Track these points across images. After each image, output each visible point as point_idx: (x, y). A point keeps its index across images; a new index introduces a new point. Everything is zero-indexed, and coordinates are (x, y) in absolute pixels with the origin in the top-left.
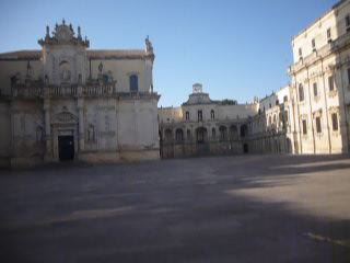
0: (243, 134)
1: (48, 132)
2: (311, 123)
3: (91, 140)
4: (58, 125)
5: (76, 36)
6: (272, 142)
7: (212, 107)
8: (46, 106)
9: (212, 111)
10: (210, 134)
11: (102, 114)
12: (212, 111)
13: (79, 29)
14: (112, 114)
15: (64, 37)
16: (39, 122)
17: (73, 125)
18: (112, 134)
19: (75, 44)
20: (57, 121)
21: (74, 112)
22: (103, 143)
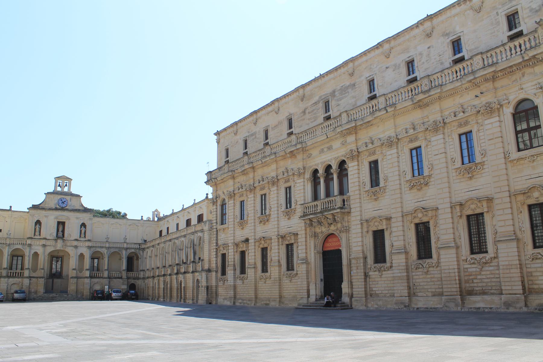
0: (130, 266)
6: (175, 285)
7: (85, 218)
9: (83, 225)
10: (73, 263)
12: (83, 225)
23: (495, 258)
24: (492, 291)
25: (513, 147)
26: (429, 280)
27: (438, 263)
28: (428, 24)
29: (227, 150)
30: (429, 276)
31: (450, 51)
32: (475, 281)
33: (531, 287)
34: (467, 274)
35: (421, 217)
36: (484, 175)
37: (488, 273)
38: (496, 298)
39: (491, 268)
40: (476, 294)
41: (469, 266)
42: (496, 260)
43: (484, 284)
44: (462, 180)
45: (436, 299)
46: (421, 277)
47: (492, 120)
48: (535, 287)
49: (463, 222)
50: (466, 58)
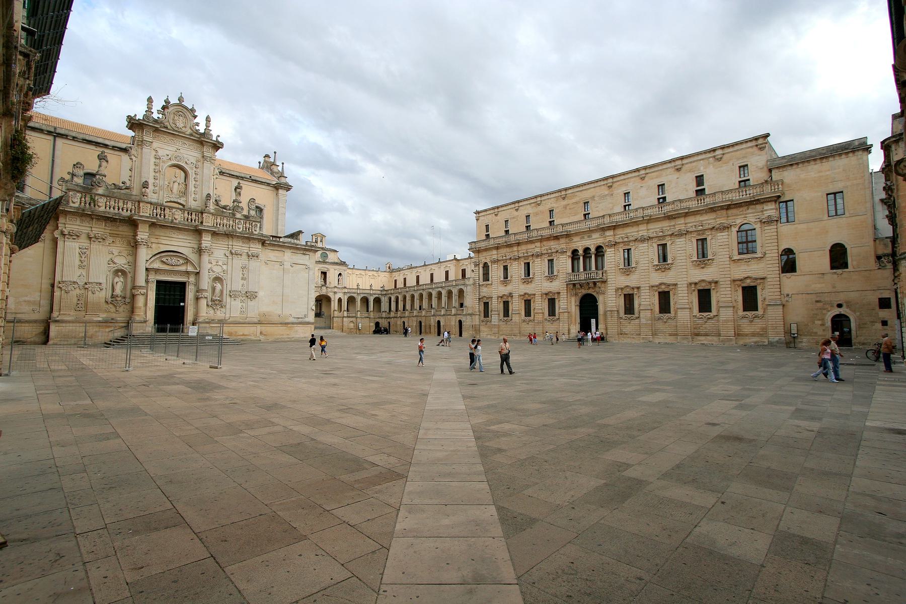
1: (141, 281)
2: (496, 306)
3: (217, 303)
4: (157, 271)
5: (201, 128)
8: (143, 234)
11: (238, 262)
13: (208, 119)
14: (253, 264)
15: (180, 124)
16: (122, 262)
17: (187, 273)
18: (251, 296)
19: (202, 143)
20: (157, 265)
21: (193, 257)
22: (234, 308)
23: (717, 315)
24: (713, 334)
25: (736, 252)
26: (667, 326)
27: (675, 317)
28: (679, 162)
29: (487, 226)
30: (667, 324)
31: (695, 183)
32: (701, 328)
33: (739, 332)
34: (696, 324)
35: (663, 288)
36: (712, 266)
37: (710, 324)
38: (715, 338)
39: (713, 321)
40: (701, 336)
41: (698, 319)
42: (717, 317)
43: (708, 330)
44: (697, 268)
45: (672, 338)
46: (661, 324)
47: (723, 234)
48: (741, 332)
49: (696, 294)
50: (707, 192)
